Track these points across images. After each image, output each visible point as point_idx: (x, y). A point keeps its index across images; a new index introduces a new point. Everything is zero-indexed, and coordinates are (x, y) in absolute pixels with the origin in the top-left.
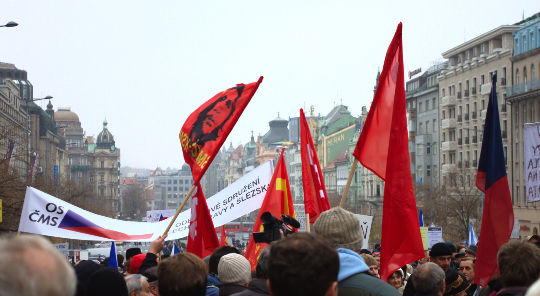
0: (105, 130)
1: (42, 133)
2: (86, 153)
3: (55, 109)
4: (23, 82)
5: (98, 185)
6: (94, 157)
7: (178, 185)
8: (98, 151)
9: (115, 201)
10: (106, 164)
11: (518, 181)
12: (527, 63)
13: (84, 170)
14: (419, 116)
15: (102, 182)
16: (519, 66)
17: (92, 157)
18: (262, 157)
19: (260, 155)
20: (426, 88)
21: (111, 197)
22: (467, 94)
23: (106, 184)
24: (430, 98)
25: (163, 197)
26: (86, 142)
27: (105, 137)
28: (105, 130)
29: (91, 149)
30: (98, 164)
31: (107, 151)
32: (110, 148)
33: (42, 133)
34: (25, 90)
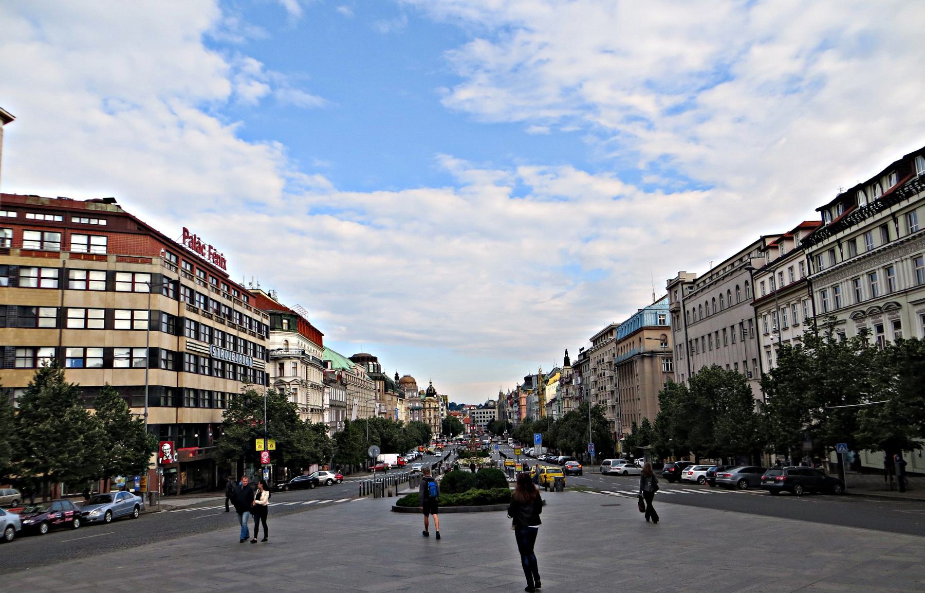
0: (431, 386)
1: (386, 390)
3: (401, 376)
6: (425, 402)
7: (482, 415)
9: (438, 426)
11: (622, 411)
12: (622, 345)
13: (419, 409)
14: (583, 374)
15: (430, 415)
16: (619, 346)
17: (423, 401)
18: (521, 398)
19: (520, 396)
20: (586, 358)
21: (435, 424)
22: (600, 362)
24: (587, 364)
26: (420, 394)
27: (431, 390)
28: (431, 386)
30: (427, 406)
31: (432, 398)
32: (433, 396)
33: (386, 390)
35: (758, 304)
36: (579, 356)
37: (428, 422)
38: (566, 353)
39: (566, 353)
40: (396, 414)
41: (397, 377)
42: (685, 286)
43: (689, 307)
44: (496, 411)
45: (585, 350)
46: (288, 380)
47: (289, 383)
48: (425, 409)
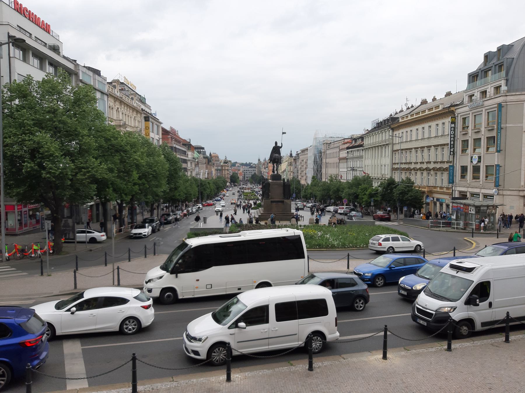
1: (208, 163)
2: (220, 165)
4: (204, 150)
5: (224, 174)
8: (224, 164)
10: (226, 168)
13: (220, 170)
15: (225, 173)
17: (222, 166)
23: (226, 174)
25: (245, 175)
26: (220, 162)
27: (226, 161)
28: (226, 158)
29: (222, 164)
30: (224, 168)
31: (226, 164)
33: (208, 163)
34: (204, 152)
35: (340, 159)
36: (296, 154)
37: (224, 176)
38: (291, 152)
39: (291, 152)
40: (212, 174)
41: (210, 155)
42: (327, 145)
43: (327, 152)
44: (256, 169)
45: (298, 153)
46: (189, 168)
47: (189, 170)
48: (222, 170)
